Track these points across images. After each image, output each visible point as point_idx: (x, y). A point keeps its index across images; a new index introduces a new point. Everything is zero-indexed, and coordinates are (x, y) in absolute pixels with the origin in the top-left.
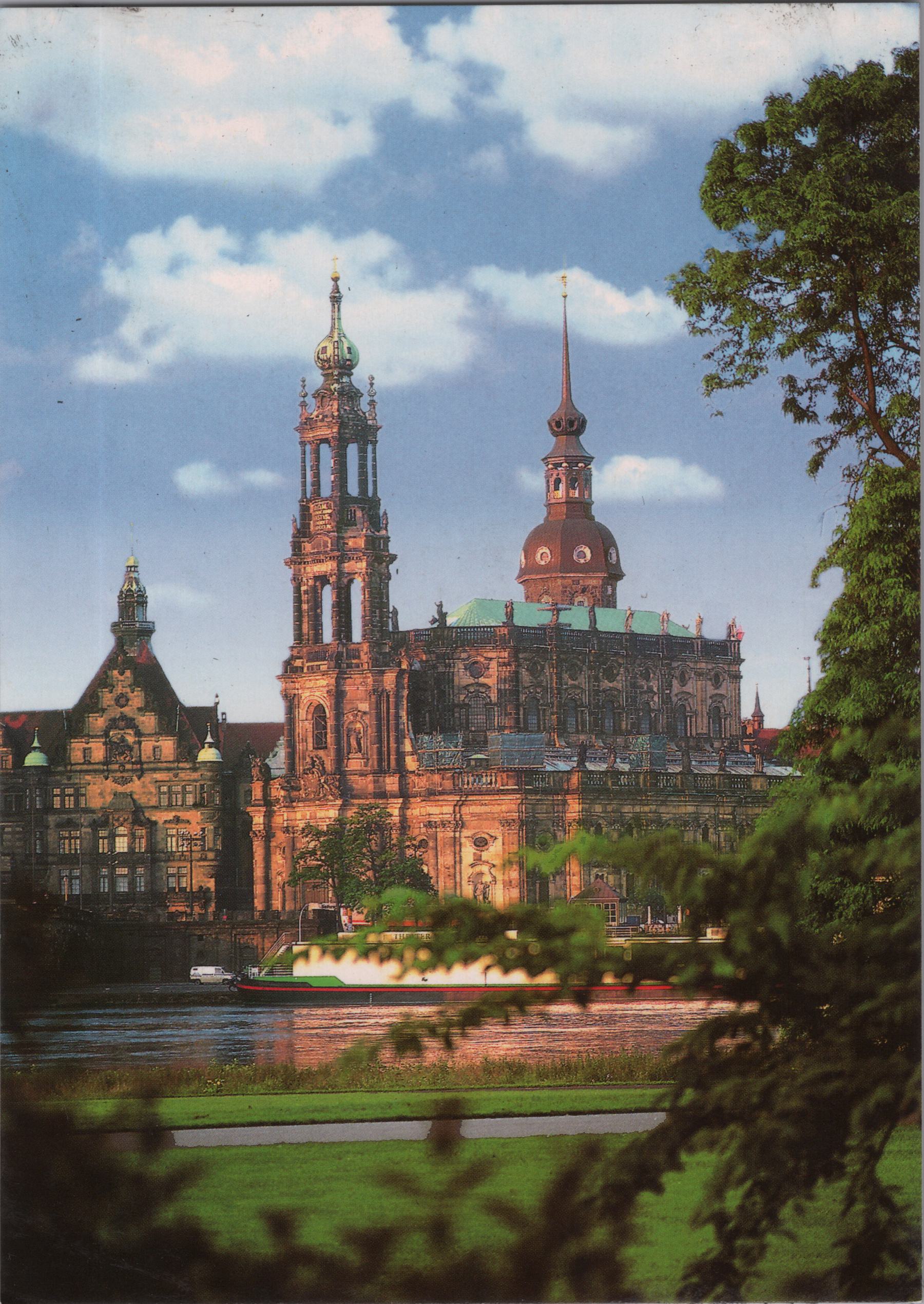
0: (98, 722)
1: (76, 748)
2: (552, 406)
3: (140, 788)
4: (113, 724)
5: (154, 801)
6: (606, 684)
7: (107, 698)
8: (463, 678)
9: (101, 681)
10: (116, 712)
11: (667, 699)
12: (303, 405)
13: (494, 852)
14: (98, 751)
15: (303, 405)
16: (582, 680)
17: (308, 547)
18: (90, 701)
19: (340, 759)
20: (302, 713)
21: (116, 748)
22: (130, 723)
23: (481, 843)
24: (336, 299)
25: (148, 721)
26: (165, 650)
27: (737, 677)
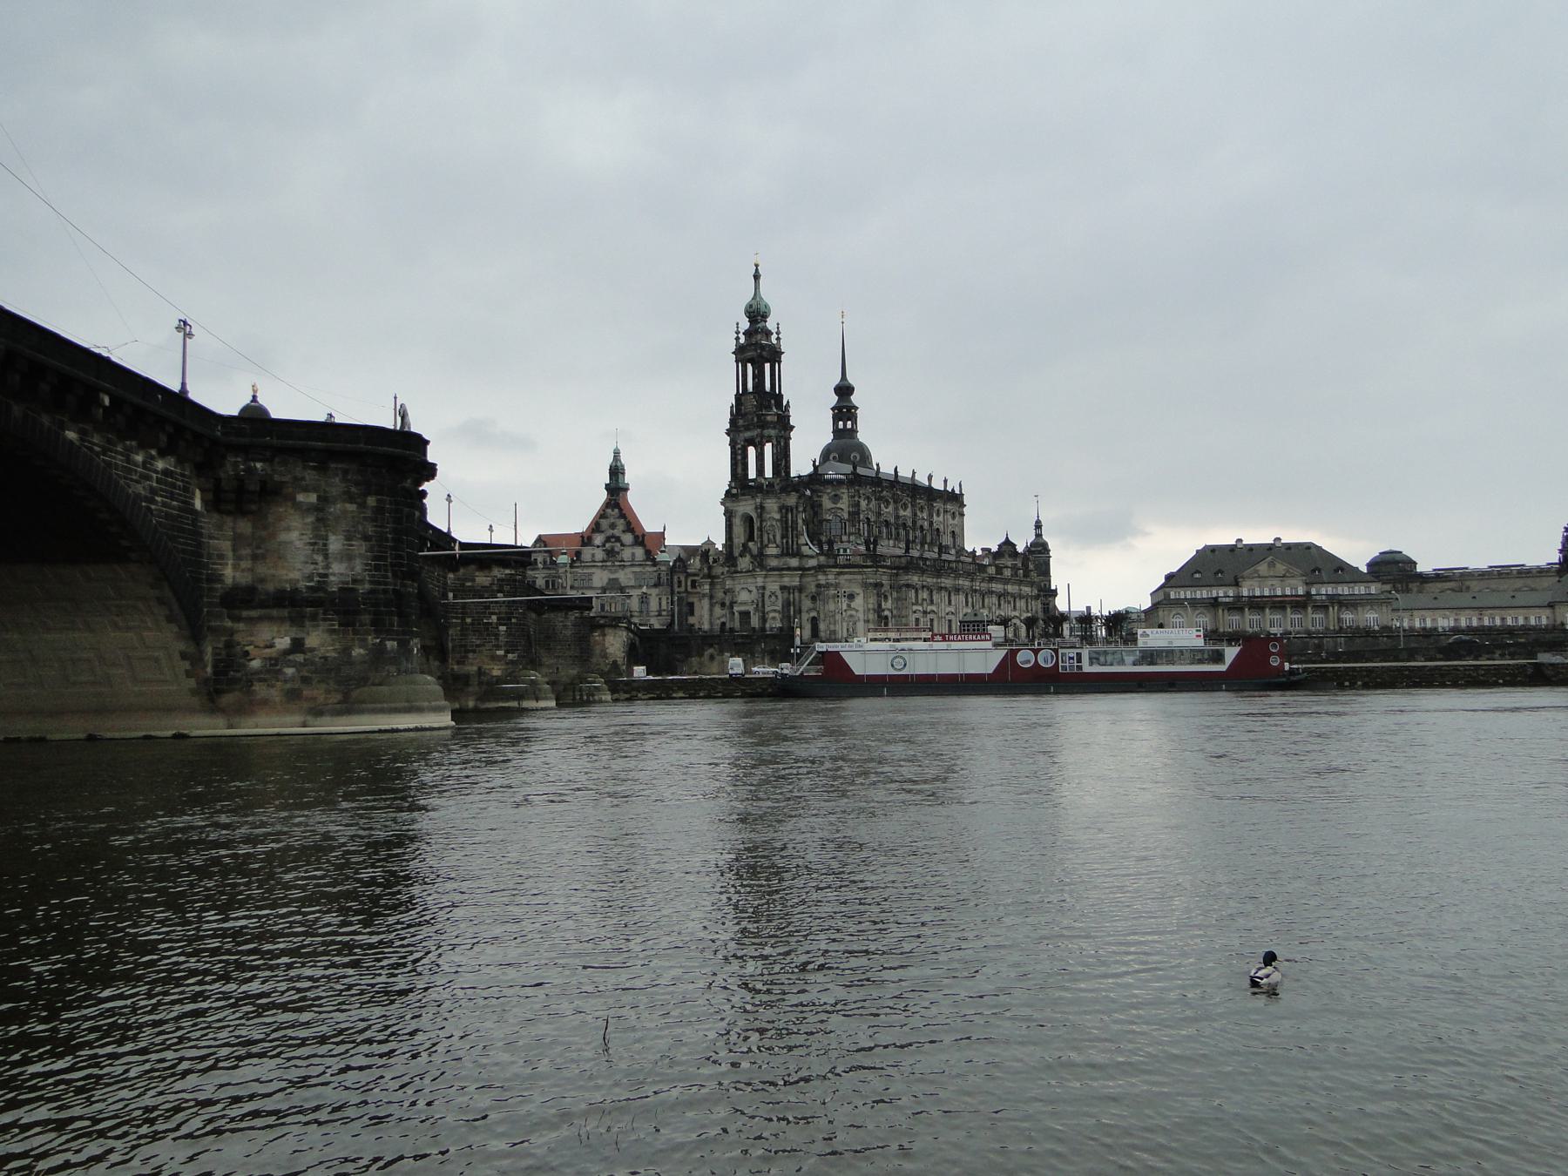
0: (598, 539)
1: (587, 553)
2: (837, 380)
3: (625, 577)
4: (608, 539)
5: (632, 583)
6: (902, 513)
7: (604, 523)
8: (827, 503)
9: (602, 515)
10: (610, 532)
11: (931, 524)
12: (737, 339)
13: (859, 602)
14: (600, 554)
15: (737, 339)
16: (891, 509)
17: (741, 422)
18: (596, 527)
19: (763, 547)
20: (737, 521)
21: (611, 553)
22: (618, 539)
23: (851, 597)
24: (757, 277)
25: (628, 538)
26: (633, 499)
27: (962, 515)
